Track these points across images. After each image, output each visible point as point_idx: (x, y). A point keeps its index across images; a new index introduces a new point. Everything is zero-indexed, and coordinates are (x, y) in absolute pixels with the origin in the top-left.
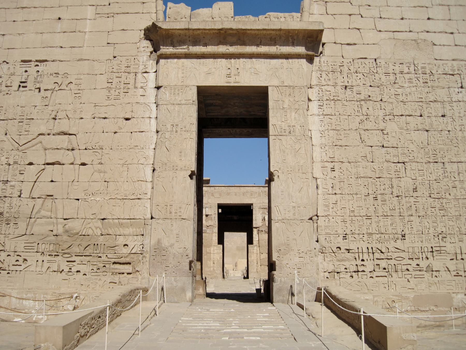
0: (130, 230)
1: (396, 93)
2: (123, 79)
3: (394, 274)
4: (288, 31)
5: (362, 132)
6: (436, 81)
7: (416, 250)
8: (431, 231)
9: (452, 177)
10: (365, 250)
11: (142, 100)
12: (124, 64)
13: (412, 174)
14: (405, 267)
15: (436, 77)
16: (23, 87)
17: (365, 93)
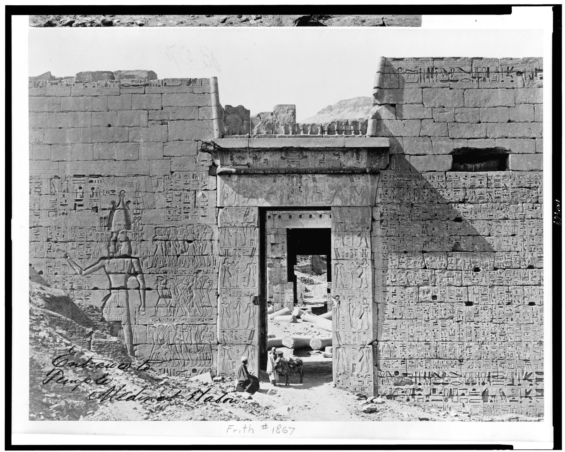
1: (465, 210)
3: (450, 399)
6: (510, 196)
9: (516, 301)
10: (422, 375)
11: (202, 221)
13: (475, 299)
15: (511, 190)
16: (79, 205)
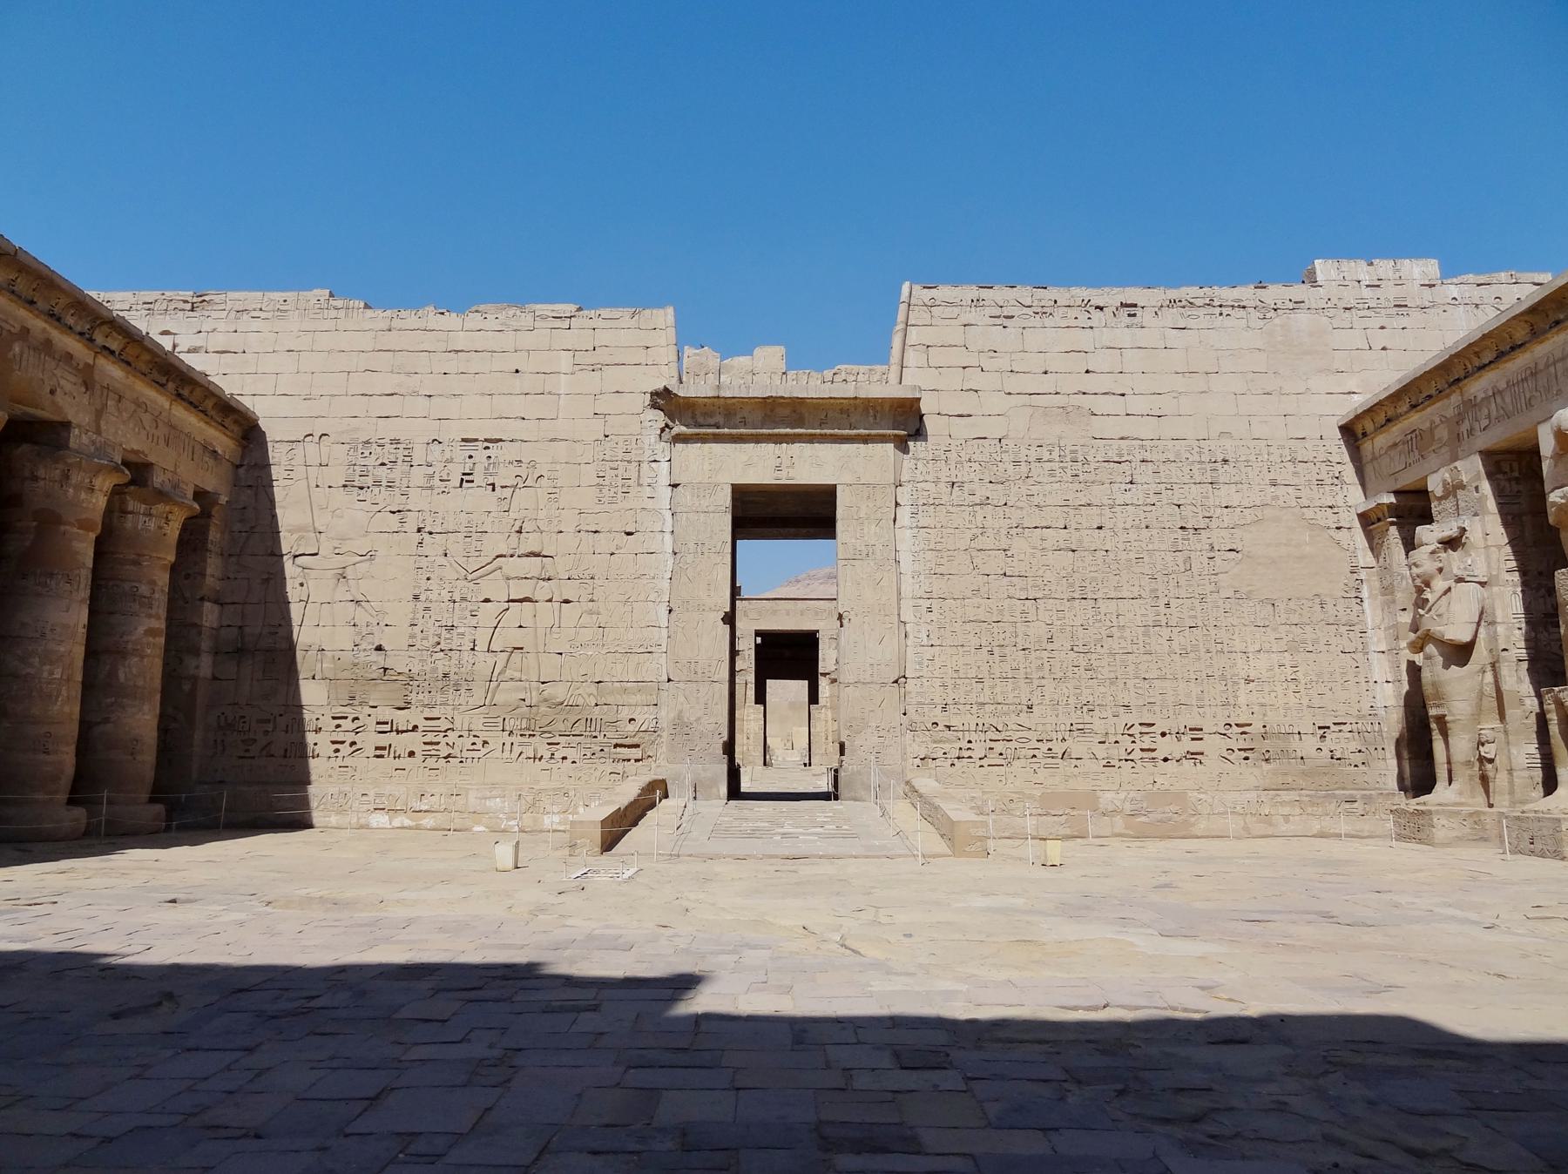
0: (638, 698)
2: (620, 472)
4: (868, 400)
5: (974, 553)
7: (1049, 727)
8: (1072, 700)
11: (650, 504)
12: (622, 447)
14: (1032, 753)
15: (1093, 465)
17: (982, 492)
